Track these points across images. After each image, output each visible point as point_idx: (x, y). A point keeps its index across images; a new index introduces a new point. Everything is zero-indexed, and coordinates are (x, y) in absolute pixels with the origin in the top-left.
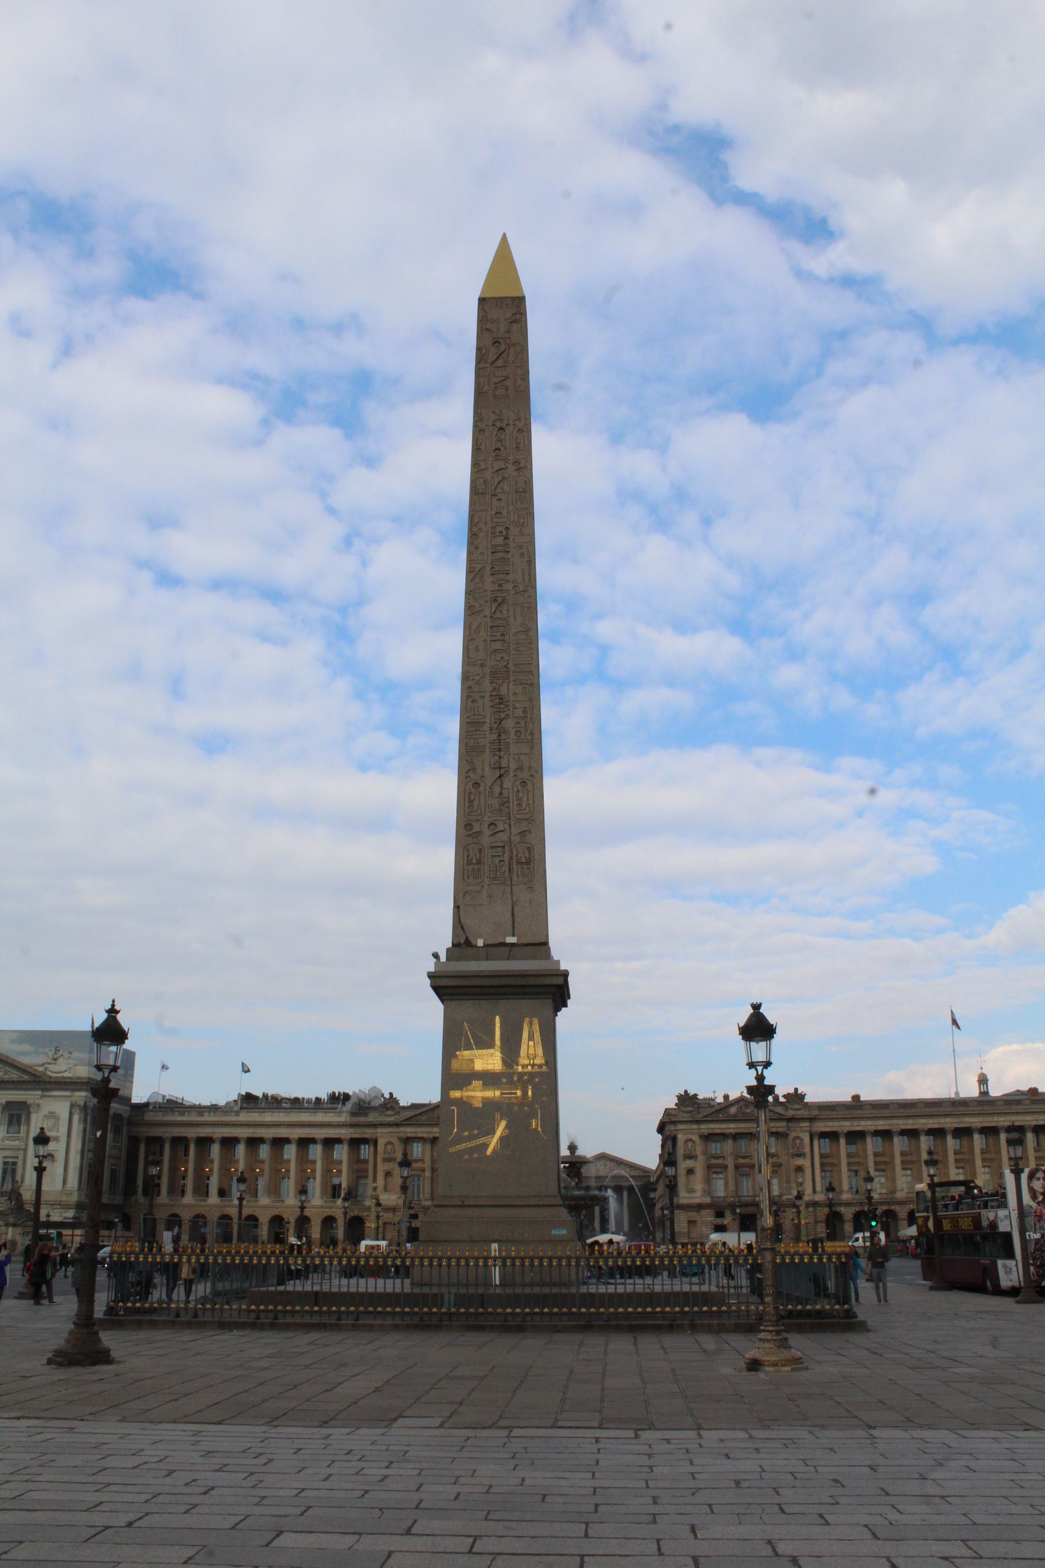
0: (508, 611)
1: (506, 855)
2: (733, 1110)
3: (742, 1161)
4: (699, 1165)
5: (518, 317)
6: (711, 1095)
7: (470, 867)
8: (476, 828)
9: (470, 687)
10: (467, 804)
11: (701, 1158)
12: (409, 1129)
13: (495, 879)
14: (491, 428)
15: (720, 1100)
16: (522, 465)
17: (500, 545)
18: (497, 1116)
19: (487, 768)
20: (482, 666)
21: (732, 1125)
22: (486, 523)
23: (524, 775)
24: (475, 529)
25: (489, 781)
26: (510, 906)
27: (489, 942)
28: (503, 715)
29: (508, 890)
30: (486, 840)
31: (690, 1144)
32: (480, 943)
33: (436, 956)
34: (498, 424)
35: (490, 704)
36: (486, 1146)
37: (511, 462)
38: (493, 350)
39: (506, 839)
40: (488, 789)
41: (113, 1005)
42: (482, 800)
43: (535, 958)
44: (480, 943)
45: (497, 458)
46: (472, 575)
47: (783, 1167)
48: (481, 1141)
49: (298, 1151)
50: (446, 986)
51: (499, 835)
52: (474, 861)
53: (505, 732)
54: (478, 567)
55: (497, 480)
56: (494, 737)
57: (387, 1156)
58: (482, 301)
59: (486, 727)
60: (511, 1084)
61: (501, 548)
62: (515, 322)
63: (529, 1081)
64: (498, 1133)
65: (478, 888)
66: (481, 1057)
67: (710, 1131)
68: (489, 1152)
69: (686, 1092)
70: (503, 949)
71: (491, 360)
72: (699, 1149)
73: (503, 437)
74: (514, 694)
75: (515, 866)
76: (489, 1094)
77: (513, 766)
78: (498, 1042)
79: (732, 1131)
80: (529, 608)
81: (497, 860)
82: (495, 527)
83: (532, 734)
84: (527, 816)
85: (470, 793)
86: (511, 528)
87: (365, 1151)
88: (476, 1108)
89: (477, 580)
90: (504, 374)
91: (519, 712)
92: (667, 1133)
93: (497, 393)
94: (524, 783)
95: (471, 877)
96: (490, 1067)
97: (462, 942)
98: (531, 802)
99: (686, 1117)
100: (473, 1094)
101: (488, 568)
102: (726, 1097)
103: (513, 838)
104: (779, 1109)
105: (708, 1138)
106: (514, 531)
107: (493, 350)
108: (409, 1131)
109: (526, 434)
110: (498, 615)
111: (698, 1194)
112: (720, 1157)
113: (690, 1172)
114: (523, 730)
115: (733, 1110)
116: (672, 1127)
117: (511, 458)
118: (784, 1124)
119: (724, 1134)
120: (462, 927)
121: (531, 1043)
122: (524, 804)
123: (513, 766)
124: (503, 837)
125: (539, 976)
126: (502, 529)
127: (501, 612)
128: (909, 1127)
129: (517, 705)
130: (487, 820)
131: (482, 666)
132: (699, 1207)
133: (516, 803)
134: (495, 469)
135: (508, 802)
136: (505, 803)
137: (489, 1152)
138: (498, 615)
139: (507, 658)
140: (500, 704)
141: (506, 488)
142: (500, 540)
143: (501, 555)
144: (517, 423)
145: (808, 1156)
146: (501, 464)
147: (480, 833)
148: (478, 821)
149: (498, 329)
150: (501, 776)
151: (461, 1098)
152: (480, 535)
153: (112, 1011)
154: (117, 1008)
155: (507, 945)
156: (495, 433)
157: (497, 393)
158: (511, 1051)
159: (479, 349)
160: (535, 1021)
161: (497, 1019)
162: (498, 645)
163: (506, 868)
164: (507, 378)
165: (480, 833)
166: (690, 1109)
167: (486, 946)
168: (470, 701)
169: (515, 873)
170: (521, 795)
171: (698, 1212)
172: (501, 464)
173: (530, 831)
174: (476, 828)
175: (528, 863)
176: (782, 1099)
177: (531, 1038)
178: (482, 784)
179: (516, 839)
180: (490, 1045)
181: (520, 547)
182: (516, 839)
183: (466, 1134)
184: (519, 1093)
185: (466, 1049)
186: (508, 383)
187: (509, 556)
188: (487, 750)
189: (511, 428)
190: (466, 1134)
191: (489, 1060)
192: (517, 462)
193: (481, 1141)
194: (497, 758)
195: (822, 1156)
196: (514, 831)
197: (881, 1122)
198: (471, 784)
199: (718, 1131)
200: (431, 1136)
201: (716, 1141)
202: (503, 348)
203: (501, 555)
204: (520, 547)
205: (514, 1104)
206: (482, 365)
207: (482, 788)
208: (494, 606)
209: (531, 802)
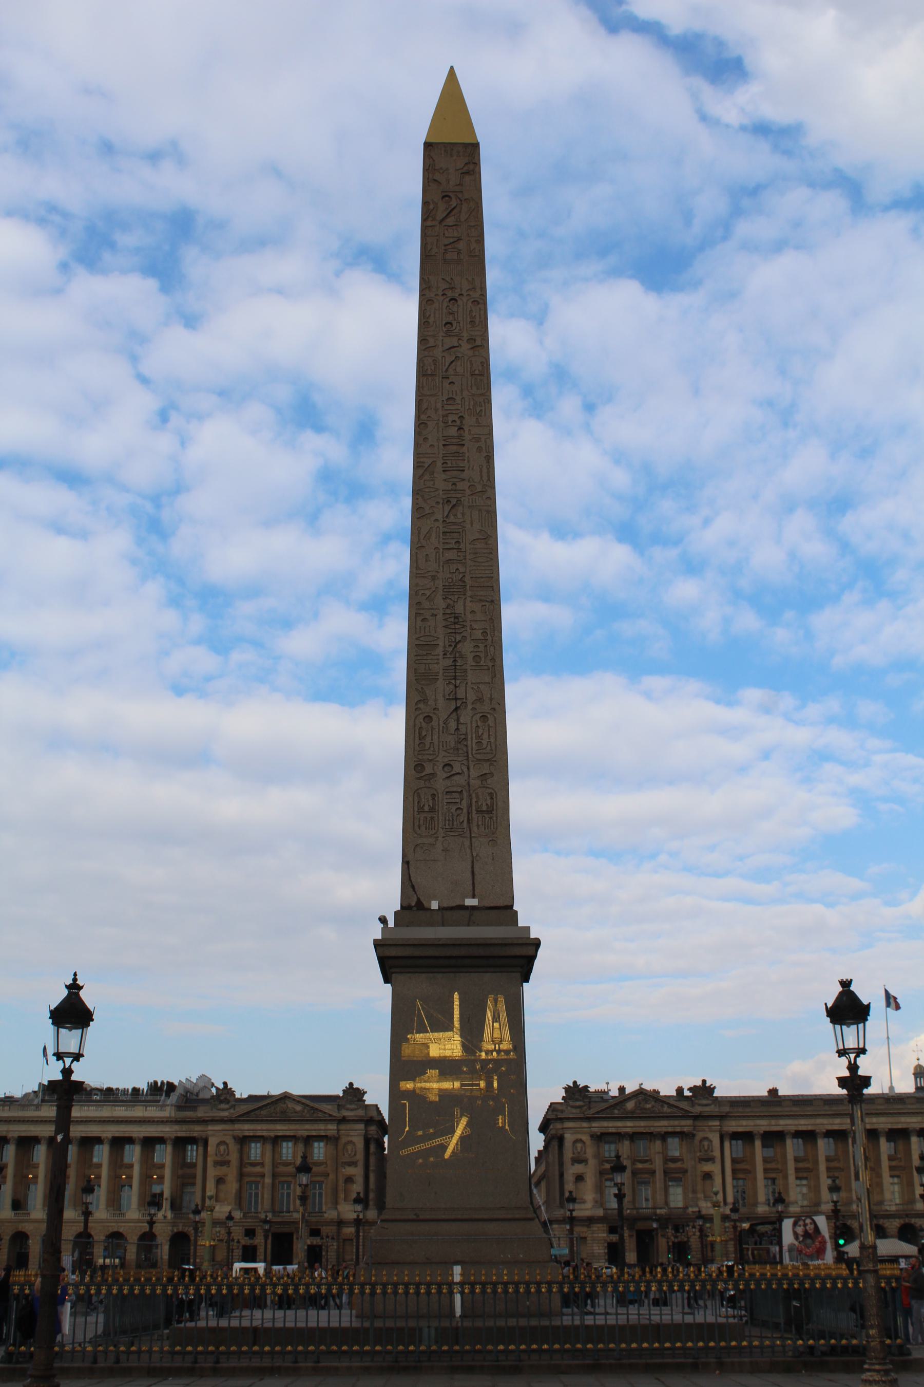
0: (463, 514)
1: (464, 802)
2: (630, 1105)
3: (640, 1166)
4: (590, 1171)
5: (471, 167)
6: (603, 1087)
7: (422, 816)
8: (428, 770)
9: (419, 603)
10: (417, 741)
11: (592, 1162)
12: (246, 1126)
13: (451, 830)
14: (441, 298)
15: (614, 1092)
16: (478, 343)
17: (453, 437)
18: (457, 1111)
19: (441, 700)
20: (434, 578)
21: (629, 1124)
22: (436, 410)
24: (423, 417)
25: (443, 716)
26: (470, 862)
27: (445, 905)
28: (458, 638)
29: (467, 843)
30: (440, 784)
31: (579, 1145)
32: (435, 905)
33: (383, 920)
34: (450, 294)
35: (444, 623)
36: (444, 1148)
37: (465, 339)
38: (442, 206)
39: (464, 783)
40: (442, 724)
41: (75, 980)
42: (435, 737)
43: (500, 924)
44: (435, 905)
45: (448, 334)
46: (421, 471)
47: (689, 1173)
48: (437, 1141)
49: (142, 1151)
50: (393, 959)
51: (456, 778)
52: (426, 808)
53: (461, 657)
54: (428, 461)
55: (449, 359)
56: (449, 662)
57: (219, 1158)
58: (428, 146)
59: (440, 651)
60: (473, 1072)
61: (454, 440)
62: (467, 173)
63: (495, 1070)
64: (458, 1132)
65: (431, 840)
66: (437, 1040)
67: (604, 1130)
68: (447, 1155)
69: (575, 1082)
70: (462, 912)
71: (440, 215)
72: (590, 1152)
73: (455, 309)
74: (473, 612)
75: (474, 815)
76: (447, 1085)
77: (471, 696)
78: (457, 1024)
79: (628, 1130)
80: (488, 512)
81: (454, 808)
82: (447, 416)
83: (493, 660)
84: (489, 756)
85: (421, 728)
86: (466, 416)
87: (192, 1153)
88: (431, 1102)
89: (427, 477)
90: (456, 234)
91: (478, 634)
92: (553, 1132)
93: (448, 256)
94: (484, 718)
95: (423, 828)
96: (448, 1053)
97: (413, 904)
98: (493, 740)
99: (575, 1113)
100: (428, 1085)
101: (439, 464)
102: (622, 1089)
103: (472, 782)
104: (684, 1105)
105: (600, 1138)
106: (469, 421)
107: (442, 206)
108: (247, 1129)
109: (481, 306)
110: (452, 519)
111: (589, 1205)
112: (646, 1161)
113: (579, 1178)
114: (482, 655)
115: (630, 1105)
116: (558, 1125)
117: (465, 335)
118: (689, 1122)
119: (619, 1134)
120: (413, 887)
121: (496, 1025)
122: (484, 742)
123: (471, 696)
124: (460, 780)
125: (506, 945)
126: (456, 418)
127: (455, 515)
128: (836, 1127)
129: (475, 626)
131: (434, 578)
132: (590, 1221)
133: (475, 741)
134: (446, 347)
135: (466, 739)
136: (462, 740)
137: (447, 1155)
138: (452, 519)
139: (462, 570)
140: (455, 623)
141: (460, 370)
142: (453, 431)
143: (454, 448)
144: (471, 293)
145: (718, 1160)
146: (454, 341)
147: (433, 775)
148: (430, 761)
149: (448, 181)
150: (457, 709)
151: (414, 1090)
152: (429, 423)
153: (74, 987)
154: (80, 982)
155: (467, 908)
156: (445, 304)
157: (448, 256)
158: (472, 1034)
159: (425, 203)
160: (501, 999)
161: (456, 995)
162: (452, 555)
163: (463, 817)
164: (459, 239)
165: (433, 775)
166: (578, 1103)
167: (441, 909)
168: (419, 619)
169: (475, 823)
170: (481, 731)
171: (588, 1226)
173: (492, 774)
174: (428, 770)
175: (489, 812)
176: (687, 1093)
177: (496, 1018)
178: (434, 717)
179: (475, 783)
180: (449, 1027)
181: (478, 440)
182: (475, 783)
183: (420, 1133)
184: (482, 1084)
185: (419, 1032)
186: (461, 245)
187: (465, 449)
188: (441, 677)
189: (465, 299)
190: (420, 1133)
191: (447, 1045)
192: (471, 340)
193: (437, 1141)
194: (452, 687)
195: (734, 1161)
196: (474, 773)
197: (803, 1122)
198: (421, 717)
199: (613, 1130)
200: (272, 1134)
201: (610, 1143)
202: (454, 203)
203: (454, 448)
204: (478, 440)
205: (477, 1098)
206: (429, 223)
207: (434, 723)
208: (447, 508)
209: (493, 740)
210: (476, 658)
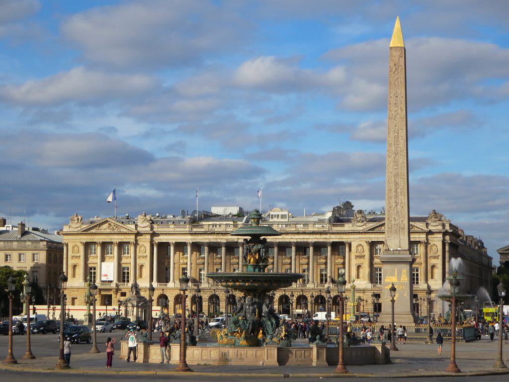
8: (390, 219)
23: (403, 205)
30: (393, 222)
34: (396, 95)
59: (393, 191)
71: (394, 71)
106: (400, 131)
130: (393, 217)
141: (398, 117)
142: (396, 134)
146: (396, 109)
147: (391, 220)
162: (396, 167)
165: (391, 220)
172: (396, 109)
174: (390, 219)
180: (394, 275)
186: (399, 80)
210: (401, 193)
